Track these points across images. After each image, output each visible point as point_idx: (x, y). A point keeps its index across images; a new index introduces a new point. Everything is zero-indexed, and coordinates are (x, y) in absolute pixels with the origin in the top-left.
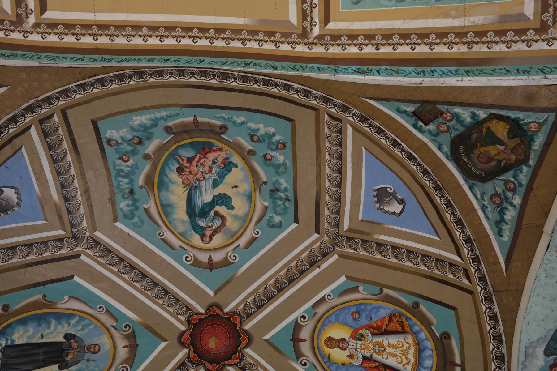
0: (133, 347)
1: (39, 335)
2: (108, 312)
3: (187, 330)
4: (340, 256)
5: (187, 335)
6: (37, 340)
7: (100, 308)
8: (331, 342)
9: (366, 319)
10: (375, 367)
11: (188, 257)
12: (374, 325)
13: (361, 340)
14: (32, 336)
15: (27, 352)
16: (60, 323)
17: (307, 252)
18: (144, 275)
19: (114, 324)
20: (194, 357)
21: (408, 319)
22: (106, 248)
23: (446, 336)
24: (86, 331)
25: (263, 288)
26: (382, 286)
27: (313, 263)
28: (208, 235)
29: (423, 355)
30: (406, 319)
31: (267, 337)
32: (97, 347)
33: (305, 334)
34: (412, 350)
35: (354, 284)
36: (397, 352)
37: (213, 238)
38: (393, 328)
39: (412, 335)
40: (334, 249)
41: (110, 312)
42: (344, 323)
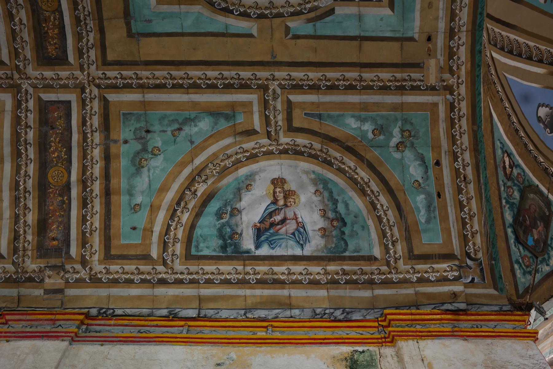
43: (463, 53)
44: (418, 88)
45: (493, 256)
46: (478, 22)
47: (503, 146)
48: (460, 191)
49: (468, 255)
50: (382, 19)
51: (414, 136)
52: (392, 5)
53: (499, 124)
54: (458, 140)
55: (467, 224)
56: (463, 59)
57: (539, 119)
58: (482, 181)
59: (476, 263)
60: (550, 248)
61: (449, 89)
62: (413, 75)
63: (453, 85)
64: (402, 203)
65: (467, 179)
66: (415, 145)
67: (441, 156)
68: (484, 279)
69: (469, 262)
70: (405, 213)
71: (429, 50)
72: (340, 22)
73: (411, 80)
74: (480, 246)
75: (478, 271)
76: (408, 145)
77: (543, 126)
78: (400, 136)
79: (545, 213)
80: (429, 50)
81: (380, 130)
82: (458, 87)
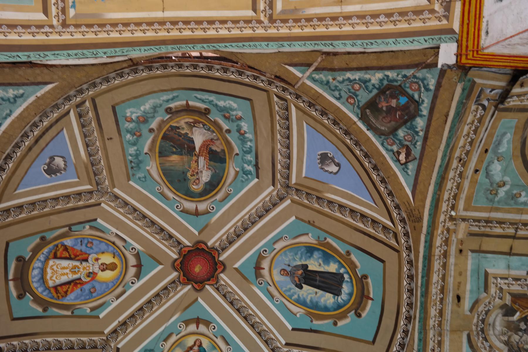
0: (258, 268)
1: (318, 295)
2: (272, 297)
3: (219, 274)
4: (103, 333)
5: (219, 270)
6: (320, 292)
7: (278, 301)
8: (112, 267)
9: (85, 290)
10: (78, 256)
11: (213, 329)
12: (79, 286)
13: (90, 273)
14: (322, 296)
15: (326, 286)
16: (304, 298)
17: (127, 332)
18: (245, 318)
19: (269, 287)
20: (215, 254)
21: (53, 298)
22: (268, 344)
23: (20, 297)
24: (288, 287)
25: (162, 303)
26: (73, 316)
27: (124, 324)
28: (196, 346)
29: (40, 276)
30: (53, 296)
31: (160, 267)
32: (282, 273)
33: (132, 271)
34: (48, 277)
35: (94, 313)
36: (60, 271)
37: (193, 343)
38: (64, 287)
39: (49, 287)
40: (107, 337)
41: (271, 296)
42: (101, 283)
43: (438, 241)
44: (475, 221)
45: (462, 106)
46: (427, 261)
47: (403, 169)
48: (467, 153)
49: (484, 108)
50: (494, 266)
51: (488, 190)
52: (486, 274)
53: (404, 184)
54: (455, 186)
55: (473, 131)
56: (439, 238)
57: (338, 165)
58: (447, 158)
59: (480, 102)
60: (377, 86)
61: (452, 218)
62: (477, 229)
63: (449, 221)
64: (519, 147)
65: (458, 160)
66: (489, 184)
67: (472, 176)
68: (482, 90)
69: (486, 103)
70: (520, 141)
71: (462, 244)
72: (523, 265)
73: (480, 226)
74: (471, 114)
75: (482, 96)
76: (495, 185)
77: (336, 160)
78: (499, 191)
79: (372, 112)
80: (462, 244)
81: (514, 197)
82: (445, 220)
